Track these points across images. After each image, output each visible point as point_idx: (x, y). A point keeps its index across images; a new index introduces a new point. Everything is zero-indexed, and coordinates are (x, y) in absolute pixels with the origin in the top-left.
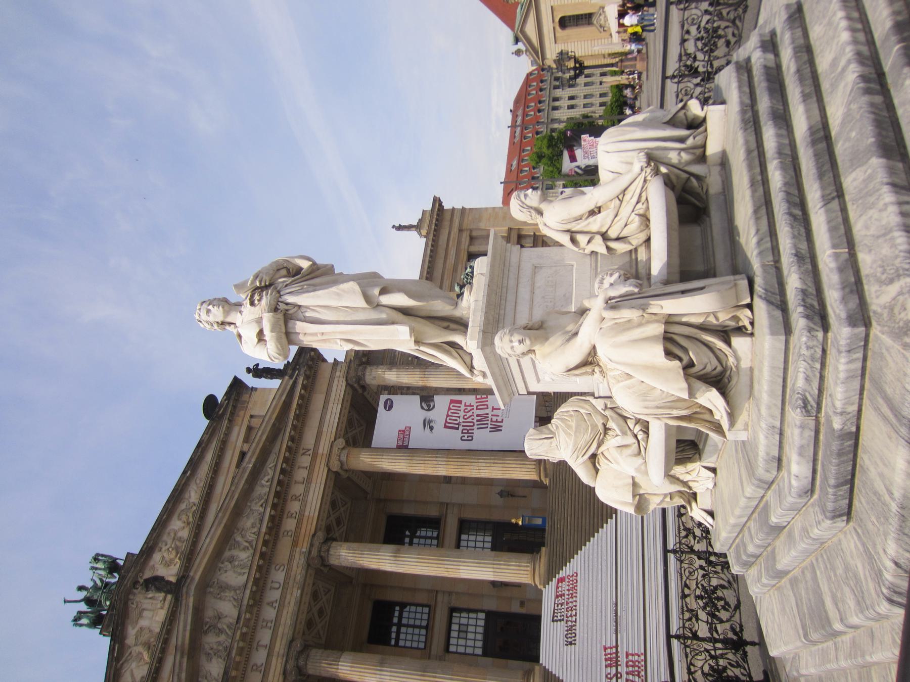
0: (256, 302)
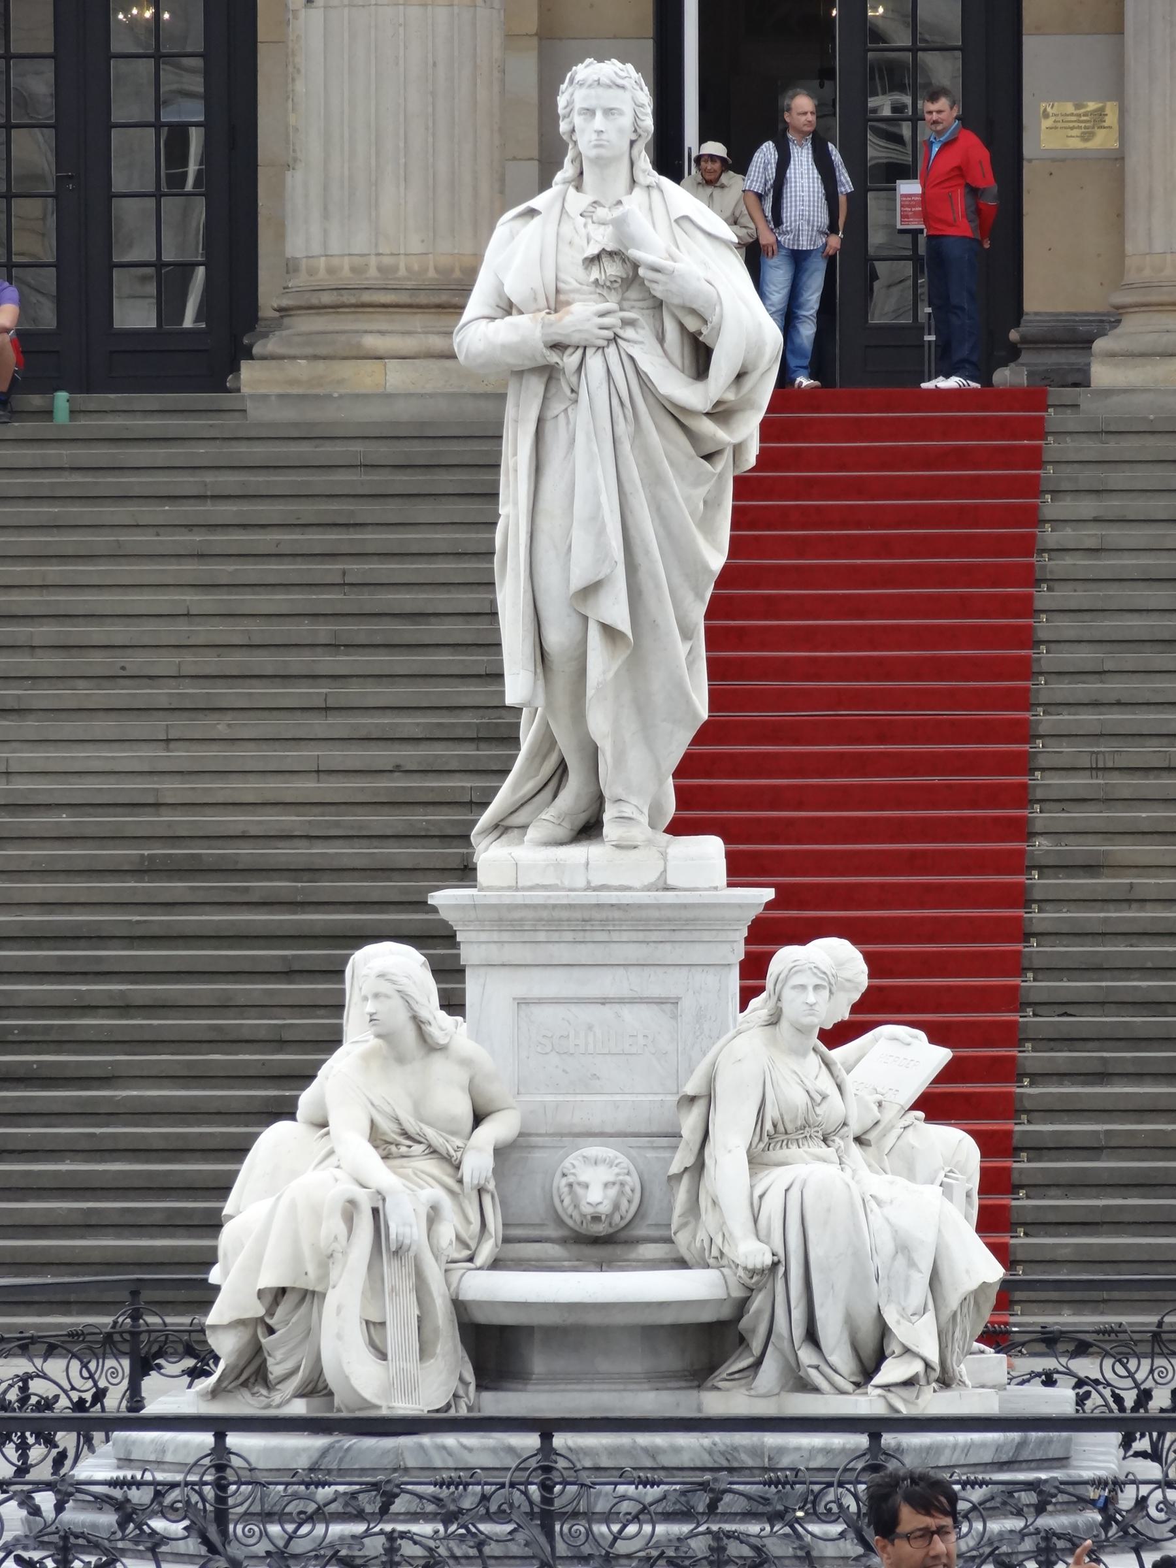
0: (595, 274)
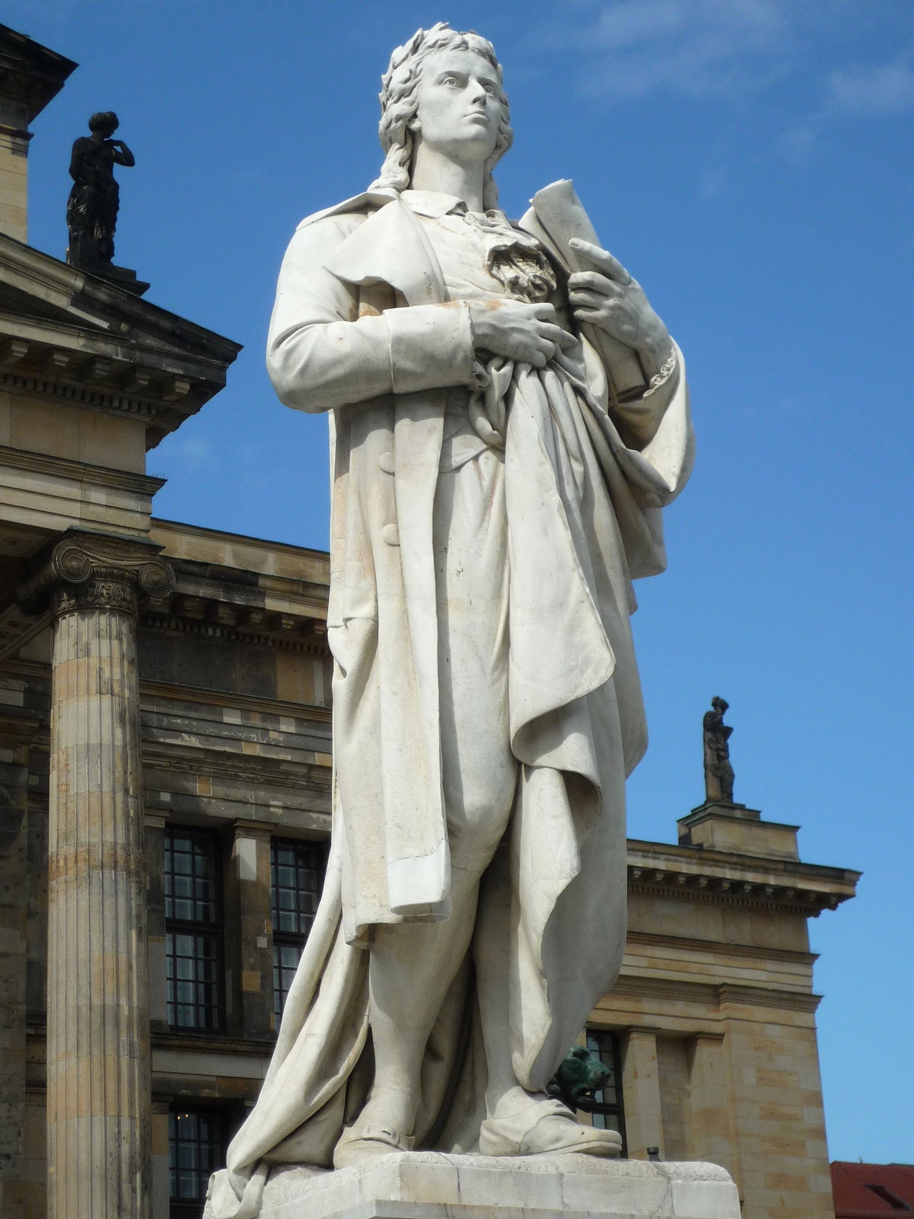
0: (508, 272)
